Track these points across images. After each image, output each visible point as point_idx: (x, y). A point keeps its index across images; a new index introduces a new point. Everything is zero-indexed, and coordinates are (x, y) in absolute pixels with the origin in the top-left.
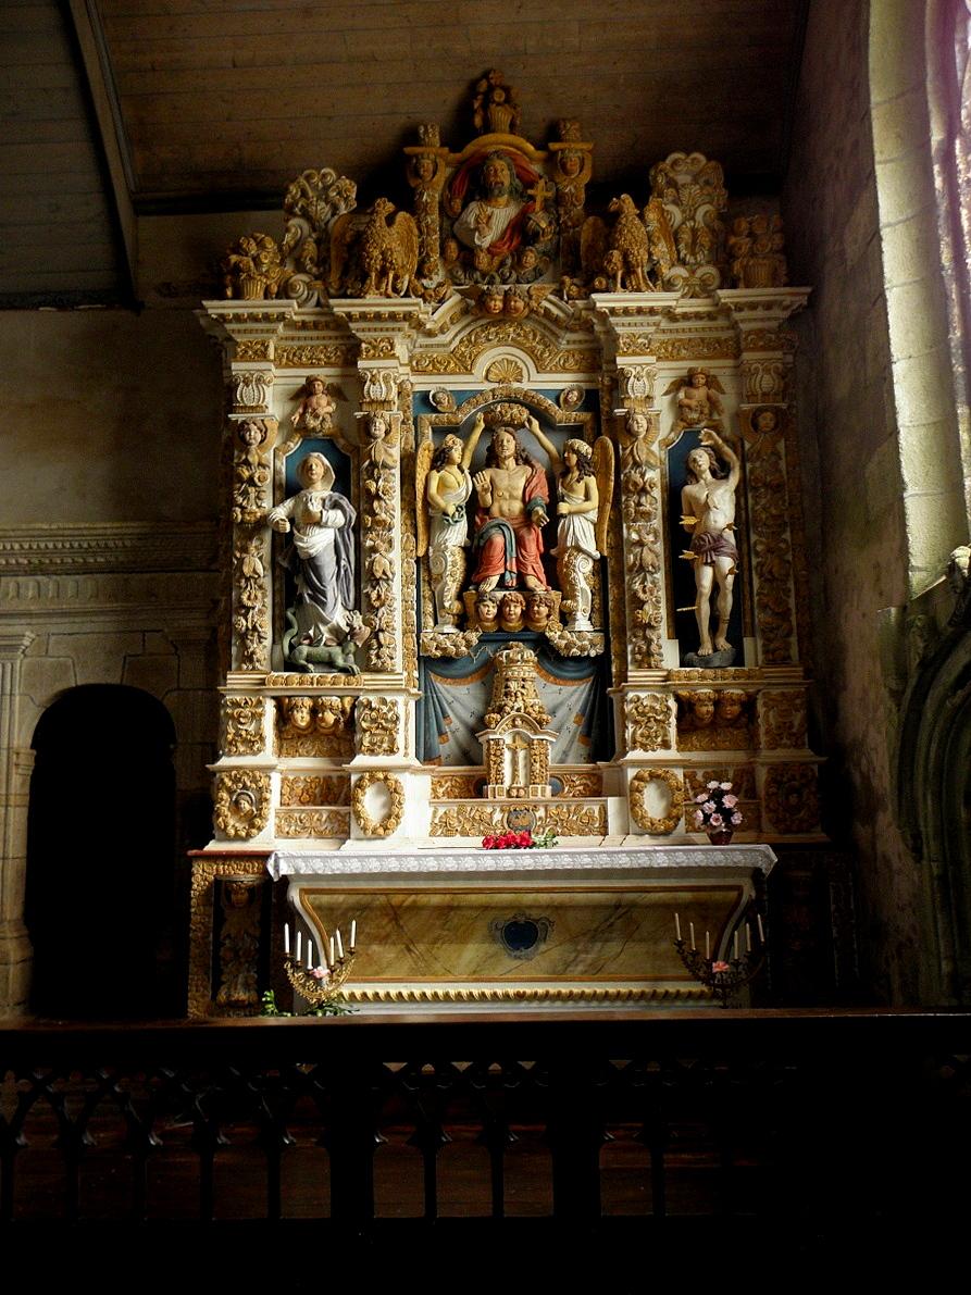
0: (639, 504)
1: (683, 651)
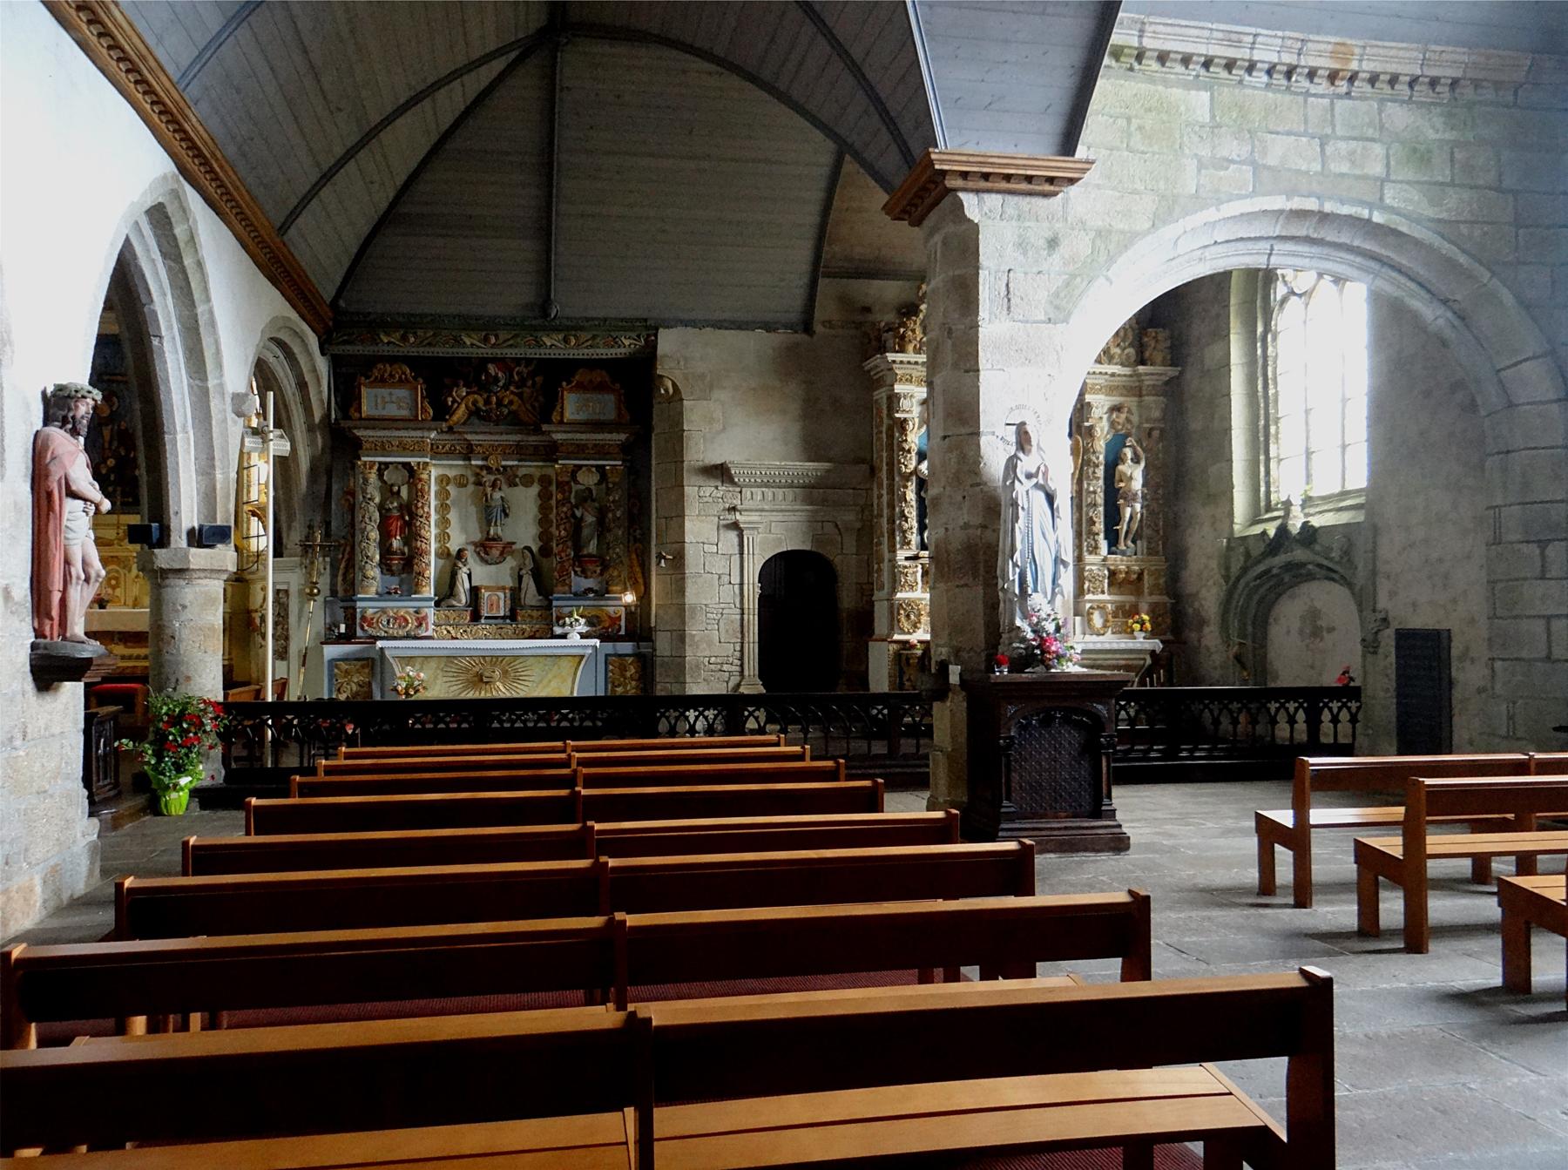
0: (1094, 472)
1: (1110, 546)
